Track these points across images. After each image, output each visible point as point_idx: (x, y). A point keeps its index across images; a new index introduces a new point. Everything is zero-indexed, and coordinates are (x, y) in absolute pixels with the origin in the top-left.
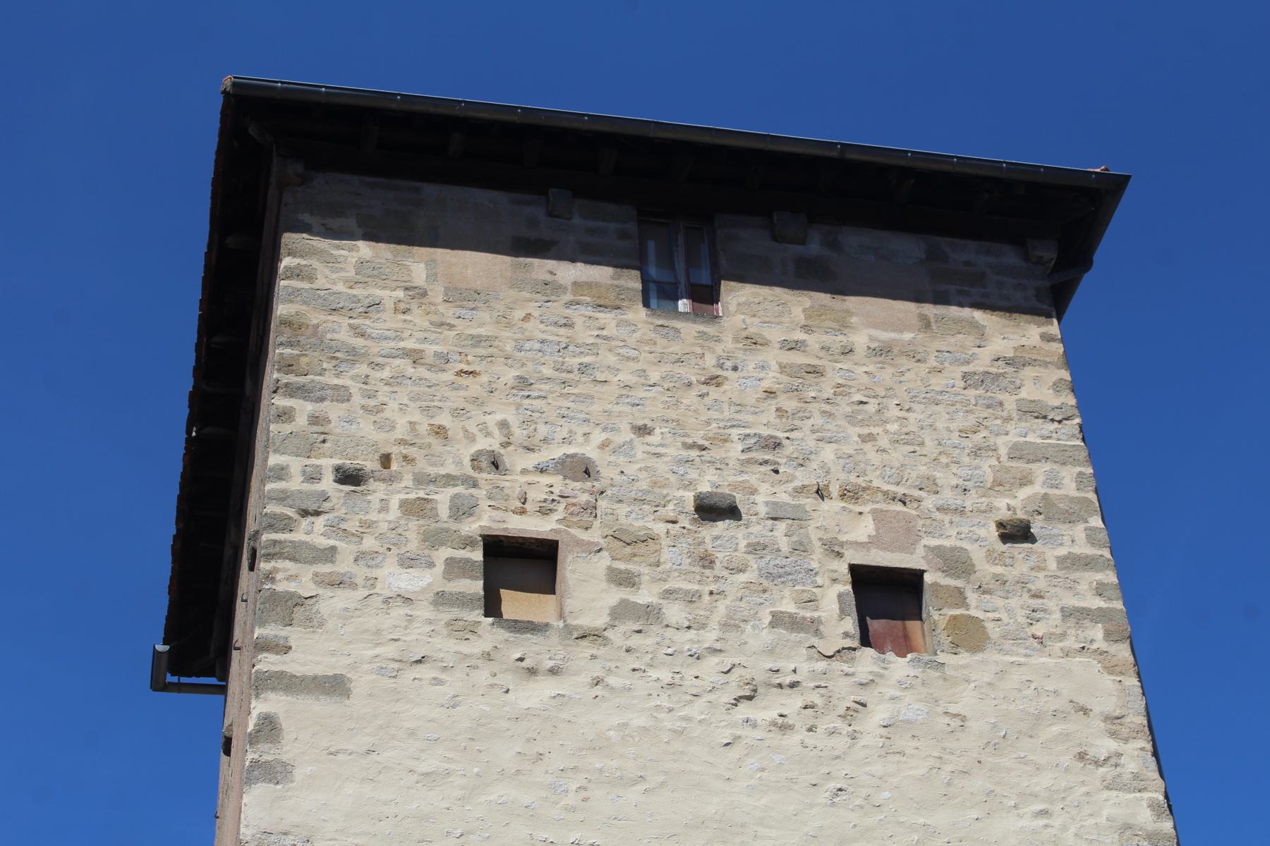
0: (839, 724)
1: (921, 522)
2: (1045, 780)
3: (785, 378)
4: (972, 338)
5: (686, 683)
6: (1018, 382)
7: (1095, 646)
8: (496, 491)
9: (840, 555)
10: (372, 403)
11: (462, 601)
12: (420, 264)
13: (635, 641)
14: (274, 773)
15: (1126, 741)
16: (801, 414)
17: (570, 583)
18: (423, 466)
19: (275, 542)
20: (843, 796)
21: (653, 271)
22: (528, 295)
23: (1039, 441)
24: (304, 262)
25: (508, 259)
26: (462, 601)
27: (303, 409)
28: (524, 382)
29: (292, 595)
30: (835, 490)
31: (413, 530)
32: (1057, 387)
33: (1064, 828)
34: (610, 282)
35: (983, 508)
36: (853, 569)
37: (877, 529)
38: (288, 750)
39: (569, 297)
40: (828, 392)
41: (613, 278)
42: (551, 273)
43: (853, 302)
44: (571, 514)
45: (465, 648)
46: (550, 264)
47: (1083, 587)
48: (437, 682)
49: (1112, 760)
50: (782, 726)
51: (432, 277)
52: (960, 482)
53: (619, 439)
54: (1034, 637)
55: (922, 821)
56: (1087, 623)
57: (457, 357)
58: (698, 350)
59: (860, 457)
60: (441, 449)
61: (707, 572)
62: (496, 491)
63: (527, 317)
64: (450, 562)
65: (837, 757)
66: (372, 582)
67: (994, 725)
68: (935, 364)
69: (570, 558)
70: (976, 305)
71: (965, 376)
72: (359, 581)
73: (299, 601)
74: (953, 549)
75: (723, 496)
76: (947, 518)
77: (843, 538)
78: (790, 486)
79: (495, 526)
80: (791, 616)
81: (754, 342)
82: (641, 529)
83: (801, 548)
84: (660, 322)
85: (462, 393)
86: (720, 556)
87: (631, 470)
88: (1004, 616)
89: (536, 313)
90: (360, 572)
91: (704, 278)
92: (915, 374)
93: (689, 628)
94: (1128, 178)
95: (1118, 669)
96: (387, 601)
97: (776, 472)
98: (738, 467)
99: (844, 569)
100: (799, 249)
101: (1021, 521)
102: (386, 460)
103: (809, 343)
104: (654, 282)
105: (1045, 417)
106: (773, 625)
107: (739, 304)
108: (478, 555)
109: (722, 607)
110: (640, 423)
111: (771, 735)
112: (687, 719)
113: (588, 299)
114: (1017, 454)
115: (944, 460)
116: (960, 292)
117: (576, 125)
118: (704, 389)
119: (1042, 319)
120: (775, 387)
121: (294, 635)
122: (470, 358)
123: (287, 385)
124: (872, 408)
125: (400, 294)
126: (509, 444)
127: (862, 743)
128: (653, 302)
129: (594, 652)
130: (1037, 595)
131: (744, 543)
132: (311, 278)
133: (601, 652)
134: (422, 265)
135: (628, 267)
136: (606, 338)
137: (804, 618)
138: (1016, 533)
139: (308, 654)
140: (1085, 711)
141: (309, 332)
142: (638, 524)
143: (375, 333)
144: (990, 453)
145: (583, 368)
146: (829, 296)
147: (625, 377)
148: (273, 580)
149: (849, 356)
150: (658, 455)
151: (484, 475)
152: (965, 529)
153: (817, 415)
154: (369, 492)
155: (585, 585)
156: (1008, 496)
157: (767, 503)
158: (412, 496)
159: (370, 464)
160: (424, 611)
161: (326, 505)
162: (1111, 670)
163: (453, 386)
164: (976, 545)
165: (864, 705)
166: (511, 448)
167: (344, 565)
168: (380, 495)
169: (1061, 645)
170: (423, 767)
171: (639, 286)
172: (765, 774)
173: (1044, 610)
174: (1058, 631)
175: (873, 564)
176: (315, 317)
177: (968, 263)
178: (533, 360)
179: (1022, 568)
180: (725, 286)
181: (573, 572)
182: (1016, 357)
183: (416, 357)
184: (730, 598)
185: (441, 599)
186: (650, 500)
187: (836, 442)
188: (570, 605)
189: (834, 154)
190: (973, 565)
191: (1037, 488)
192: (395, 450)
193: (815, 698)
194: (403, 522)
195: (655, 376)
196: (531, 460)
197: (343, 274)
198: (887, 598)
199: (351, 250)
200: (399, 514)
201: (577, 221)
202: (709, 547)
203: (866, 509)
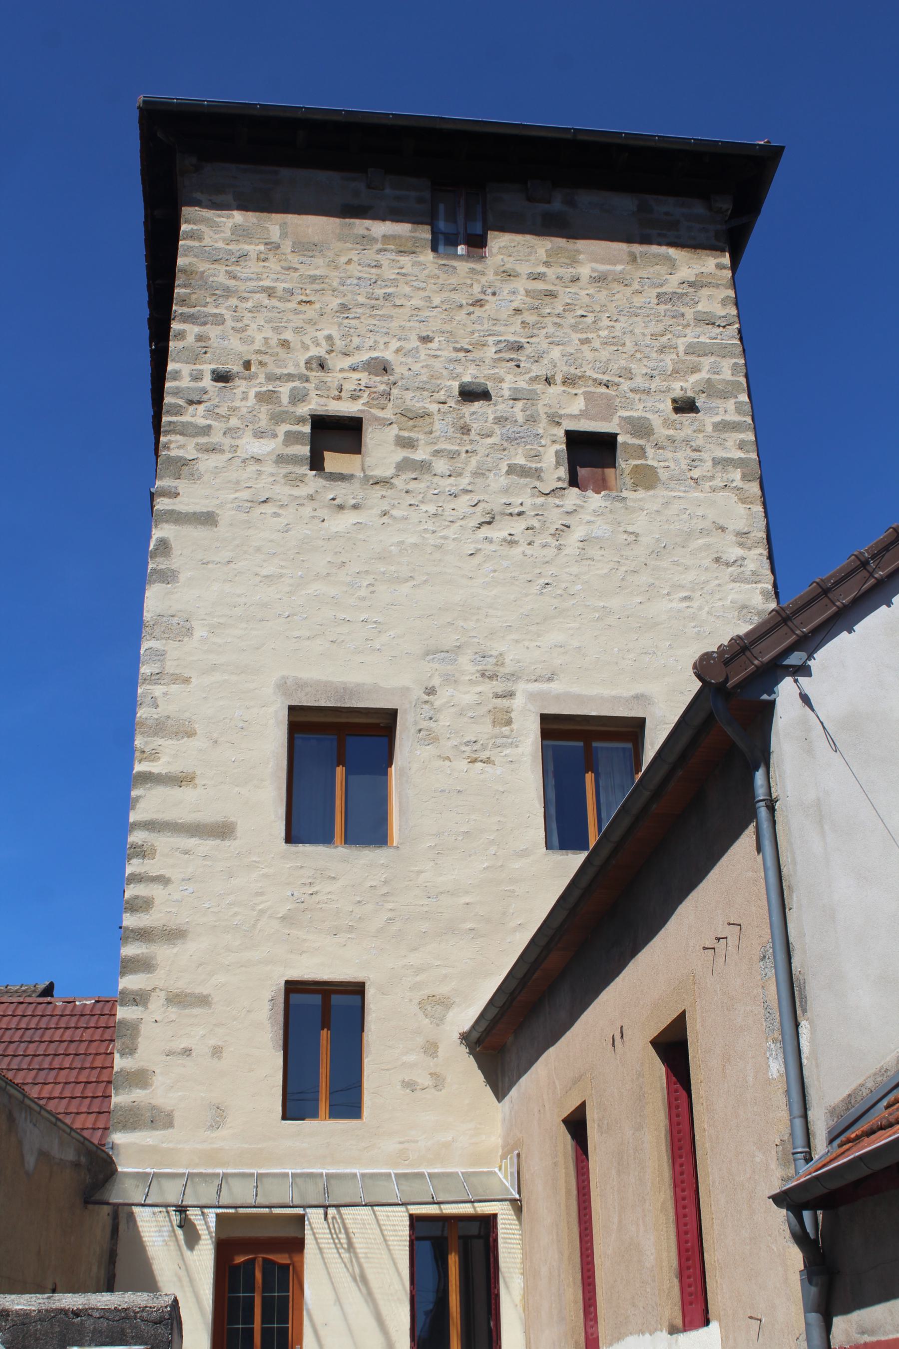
0: (550, 540)
1: (618, 400)
2: (691, 576)
3: (529, 300)
4: (665, 268)
5: (446, 513)
6: (696, 299)
7: (734, 484)
8: (322, 385)
9: (559, 424)
10: (239, 325)
11: (294, 460)
12: (275, 225)
13: (413, 485)
14: (167, 577)
15: (750, 549)
16: (539, 325)
17: (369, 446)
18: (272, 368)
19: (170, 423)
20: (549, 588)
21: (442, 225)
22: (351, 246)
23: (708, 341)
24: (195, 227)
25: (337, 220)
26: (294, 460)
27: (192, 330)
28: (344, 308)
30: (559, 379)
32: (724, 302)
33: (700, 608)
34: (408, 234)
35: (664, 389)
36: (568, 433)
37: (586, 407)
38: (175, 562)
39: (379, 246)
40: (559, 309)
41: (411, 231)
42: (368, 229)
43: (581, 244)
44: (373, 399)
45: (296, 492)
46: (367, 223)
47: (730, 444)
48: (276, 515)
49: (739, 562)
50: (511, 542)
51: (284, 235)
52: (649, 371)
53: (408, 346)
54: (692, 478)
55: (602, 604)
56: (730, 468)
57: (299, 291)
58: (469, 282)
59: (579, 355)
60: (285, 356)
61: (465, 437)
62: (322, 385)
63: (349, 261)
65: (547, 562)
67: (658, 540)
68: (638, 287)
69: (370, 429)
70: (671, 244)
71: (658, 296)
72: (226, 448)
73: (184, 463)
74: (639, 418)
75: (479, 384)
76: (637, 397)
77: (562, 412)
79: (319, 408)
80: (521, 466)
81: (509, 275)
82: (420, 408)
83: (532, 419)
84: (443, 262)
85: (301, 316)
86: (475, 426)
87: (416, 367)
88: (672, 464)
89: (355, 258)
90: (227, 442)
91: (479, 230)
92: (623, 295)
93: (450, 476)
94: (782, 148)
95: (749, 500)
97: (518, 366)
98: (492, 364)
99: (561, 433)
100: (547, 206)
101: (689, 398)
102: (247, 365)
103: (548, 274)
104: (442, 233)
105: (713, 324)
106: (508, 473)
107: (500, 248)
108: (307, 429)
109: (474, 461)
110: (424, 334)
111: (502, 548)
112: (445, 538)
113: (393, 247)
114: (691, 351)
115: (638, 355)
116: (659, 235)
118: (471, 309)
119: (718, 253)
120: (521, 307)
121: (182, 485)
122: (308, 292)
123: (181, 314)
124: (589, 320)
125: (262, 247)
126: (332, 351)
127: (565, 552)
128: (441, 248)
129: (384, 493)
131: (493, 416)
133: (389, 493)
134: (278, 227)
135: (422, 223)
136: (404, 275)
137: (531, 468)
138: (685, 406)
139: (189, 497)
140: (723, 529)
141: (197, 277)
142: (418, 405)
143: (243, 276)
144: (672, 350)
145: (387, 297)
146: (564, 240)
147: (415, 302)
148: (168, 449)
149: (577, 283)
150: (436, 356)
151: (314, 373)
152: (649, 404)
153: (550, 325)
154: (235, 387)
155: (380, 448)
156: (682, 380)
157: (510, 389)
158: (264, 389)
159: (236, 368)
160: (269, 468)
161: (205, 397)
162: (743, 501)
163: (296, 312)
164: (656, 415)
165: (568, 527)
166: (333, 354)
167: (216, 438)
168: (242, 389)
169: (711, 484)
170: (265, 572)
171: (429, 236)
172: (496, 574)
173: (701, 460)
174: (709, 474)
175: (582, 429)
176: (202, 266)
177: (667, 214)
178: (352, 292)
179: (687, 431)
180: (491, 235)
181: (372, 439)
183: (270, 292)
184: (479, 455)
185: (281, 459)
186: (428, 388)
187: (562, 344)
188: (369, 461)
189: (569, 136)
190: (653, 430)
191: (704, 375)
192: (254, 358)
193: (535, 523)
194: (257, 407)
195: (436, 301)
196: (347, 362)
197: (222, 235)
198: (590, 454)
199: (228, 217)
200: (254, 401)
201: (388, 191)
202: (468, 420)
203: (579, 391)
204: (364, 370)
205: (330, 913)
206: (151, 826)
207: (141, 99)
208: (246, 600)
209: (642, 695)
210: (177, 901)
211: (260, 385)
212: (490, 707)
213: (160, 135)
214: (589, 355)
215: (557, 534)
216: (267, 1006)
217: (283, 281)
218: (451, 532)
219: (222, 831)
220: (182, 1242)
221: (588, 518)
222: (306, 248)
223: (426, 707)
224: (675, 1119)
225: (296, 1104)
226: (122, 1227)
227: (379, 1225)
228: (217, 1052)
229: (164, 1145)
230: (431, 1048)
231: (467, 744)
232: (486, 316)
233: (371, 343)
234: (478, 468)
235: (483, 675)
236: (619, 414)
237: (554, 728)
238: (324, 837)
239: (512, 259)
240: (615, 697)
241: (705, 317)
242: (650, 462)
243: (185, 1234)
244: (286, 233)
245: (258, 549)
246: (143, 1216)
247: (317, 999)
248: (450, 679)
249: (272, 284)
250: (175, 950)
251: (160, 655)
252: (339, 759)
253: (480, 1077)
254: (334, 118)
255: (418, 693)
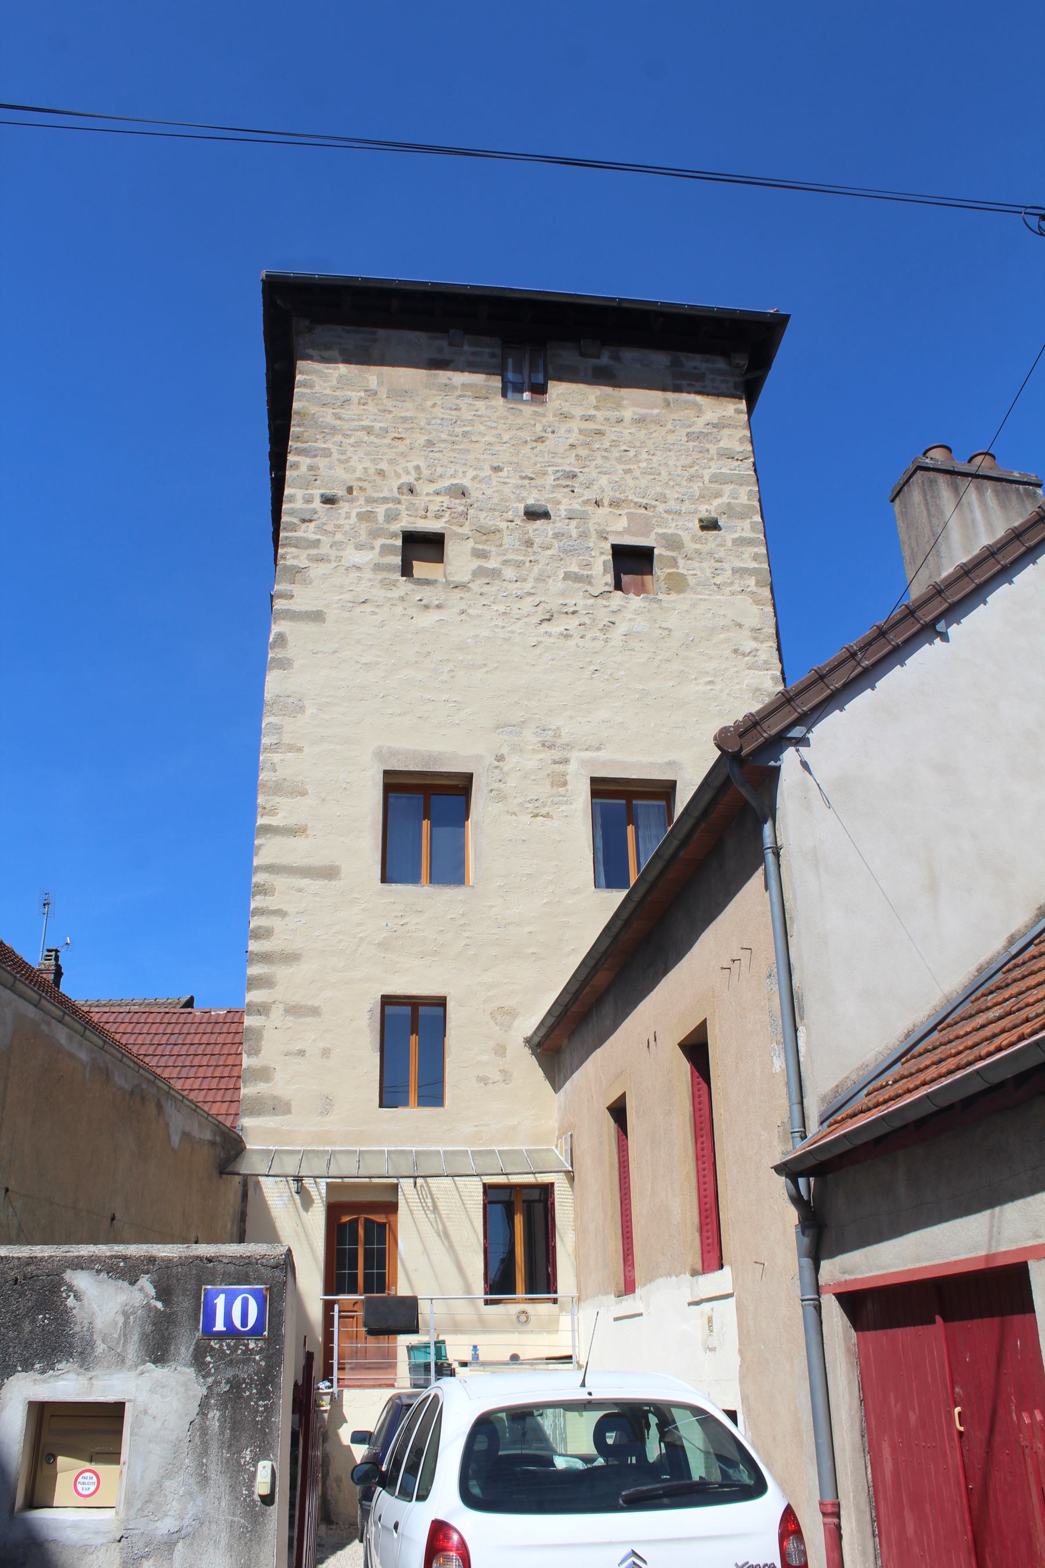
0: (599, 634)
3: (582, 437)
9: (606, 538)
10: (344, 457)
11: (388, 568)
12: (373, 376)
13: (486, 589)
14: (284, 664)
15: (762, 642)
19: (287, 538)
20: (597, 674)
21: (510, 376)
26: (388, 568)
27: (304, 462)
28: (430, 443)
29: (295, 567)
30: (606, 502)
31: (363, 529)
32: (741, 440)
33: (722, 691)
34: (483, 383)
38: (290, 652)
39: (459, 393)
40: (607, 445)
43: (625, 392)
45: (390, 594)
46: (449, 373)
47: (746, 556)
48: (374, 613)
50: (566, 636)
51: (380, 383)
53: (483, 474)
56: (746, 576)
58: (533, 422)
61: (529, 549)
64: (383, 546)
66: (339, 559)
72: (333, 558)
73: (299, 570)
74: (672, 535)
75: (540, 506)
76: (670, 517)
78: (580, 500)
79: (409, 525)
80: (575, 573)
81: (565, 417)
83: (584, 535)
85: (395, 450)
87: (489, 492)
88: (698, 572)
89: (439, 403)
90: (333, 553)
91: (540, 378)
96: (346, 569)
100: (596, 361)
102: (350, 490)
106: (564, 579)
109: (536, 570)
110: (496, 465)
112: (512, 632)
115: (671, 483)
116: (689, 385)
117: (463, 291)
118: (534, 445)
121: (295, 589)
124: (631, 454)
125: (362, 394)
128: (510, 394)
130: (719, 561)
132: (312, 387)
133: (467, 595)
136: (479, 416)
138: (710, 525)
140: (740, 626)
143: (347, 417)
145: (465, 434)
147: (489, 439)
148: (285, 559)
150: (505, 483)
152: (680, 523)
153: (599, 458)
158: (364, 510)
159: (340, 492)
160: (368, 574)
161: (315, 516)
162: (757, 602)
163: (390, 446)
167: (324, 550)
168: (346, 509)
170: (363, 660)
176: (314, 409)
177: (695, 368)
179: (711, 546)
180: (550, 384)
182: (716, 421)
185: (378, 567)
188: (450, 569)
189: (615, 304)
191: (725, 499)
192: (355, 484)
196: (432, 488)
198: (632, 562)
199: (335, 369)
201: (466, 348)
204: (446, 494)
205: (417, 941)
206: (270, 869)
207: (263, 274)
208: (348, 682)
209: (674, 762)
210: (292, 930)
211: (360, 506)
212: (549, 771)
213: (279, 302)
214: (631, 483)
215: (604, 629)
216: (367, 1016)
217: (379, 421)
218: (517, 627)
219: (330, 873)
220: (299, 1205)
221: (630, 616)
222: (398, 394)
223: (497, 771)
224: (698, 1106)
225: (391, 1095)
226: (250, 1193)
227: (459, 1192)
228: (326, 1053)
229: (284, 1128)
230: (501, 1050)
231: (530, 801)
232: (546, 450)
233: (452, 472)
234: (540, 575)
235: (543, 745)
236: (656, 530)
237: (603, 790)
238: (413, 878)
239: (568, 404)
240: (651, 764)
241: (726, 452)
242: (680, 571)
243: (301, 1198)
244: (382, 382)
245: (358, 642)
246: (266, 1183)
247: (407, 1010)
248: (516, 749)
249: (371, 424)
250: (292, 970)
251: (278, 729)
252: (425, 813)
253: (540, 1072)
254: (421, 288)
255: (490, 760)
